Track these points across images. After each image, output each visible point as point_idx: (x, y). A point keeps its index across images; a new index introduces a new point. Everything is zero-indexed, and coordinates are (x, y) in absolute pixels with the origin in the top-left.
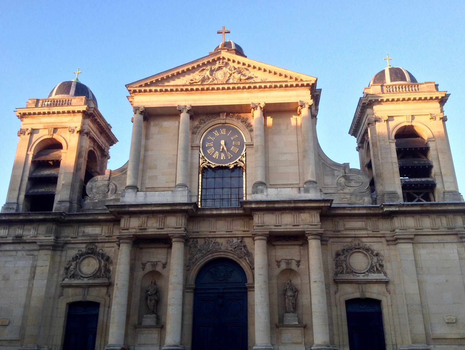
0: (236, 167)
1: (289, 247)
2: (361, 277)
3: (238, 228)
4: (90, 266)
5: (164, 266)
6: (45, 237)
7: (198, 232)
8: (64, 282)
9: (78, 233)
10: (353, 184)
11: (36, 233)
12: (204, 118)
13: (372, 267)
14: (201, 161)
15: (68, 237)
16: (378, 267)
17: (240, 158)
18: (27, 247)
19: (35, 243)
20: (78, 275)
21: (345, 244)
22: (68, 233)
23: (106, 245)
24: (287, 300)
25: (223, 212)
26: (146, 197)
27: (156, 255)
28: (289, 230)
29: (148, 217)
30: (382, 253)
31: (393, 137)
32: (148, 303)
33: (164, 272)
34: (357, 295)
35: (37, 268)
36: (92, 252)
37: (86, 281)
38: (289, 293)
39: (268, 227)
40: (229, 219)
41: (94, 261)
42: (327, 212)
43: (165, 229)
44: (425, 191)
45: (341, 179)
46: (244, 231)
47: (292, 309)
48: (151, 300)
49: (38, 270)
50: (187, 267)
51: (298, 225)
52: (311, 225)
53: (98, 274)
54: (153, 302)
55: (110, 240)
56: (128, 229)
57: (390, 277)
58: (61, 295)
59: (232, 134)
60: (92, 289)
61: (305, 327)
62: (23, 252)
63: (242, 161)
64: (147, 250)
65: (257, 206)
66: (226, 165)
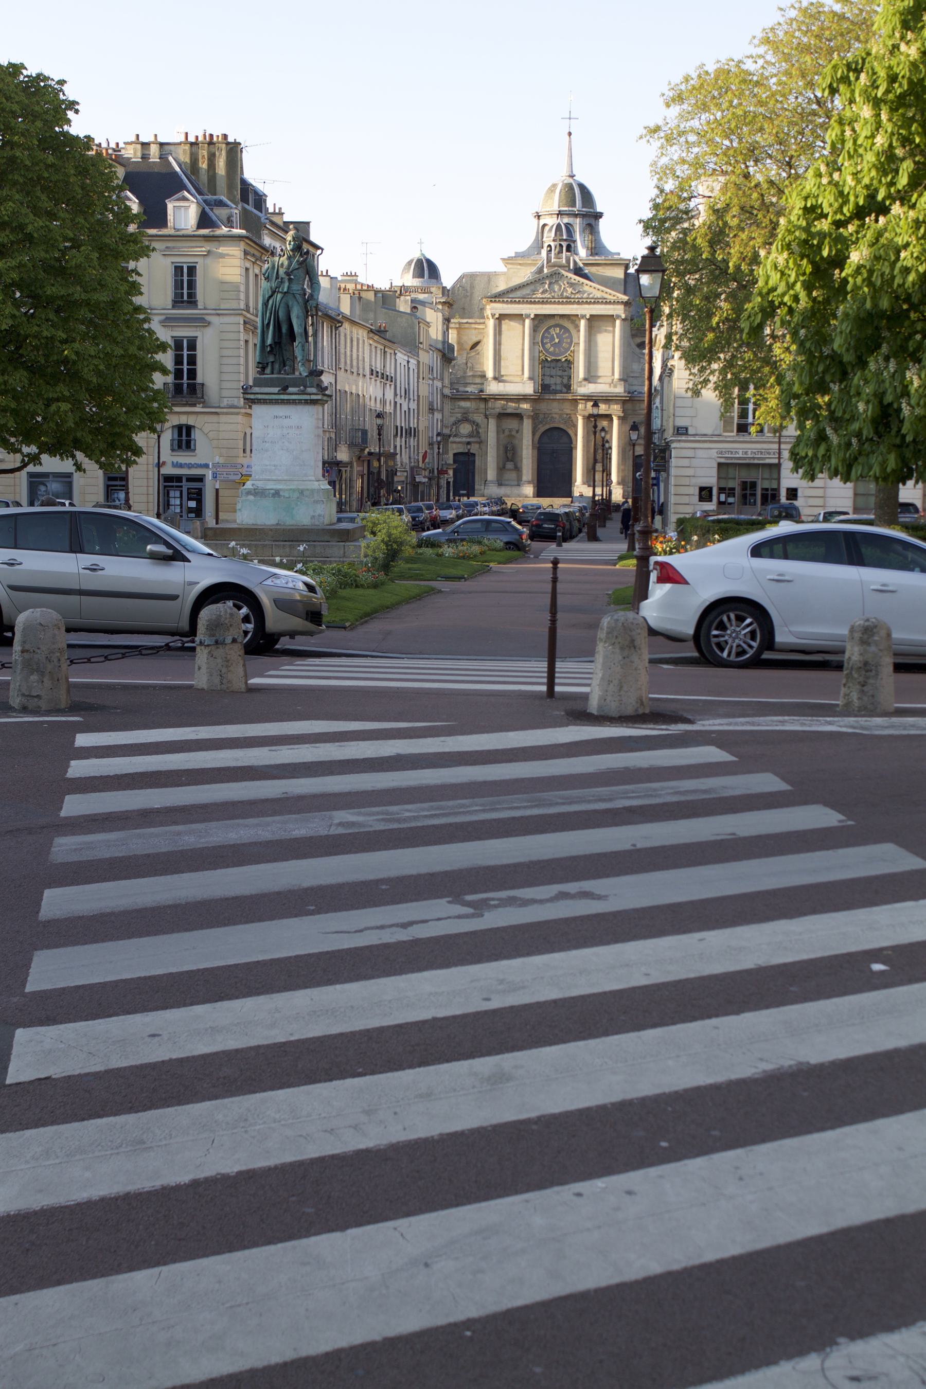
4: (465, 429)
5: (517, 432)
27: (512, 424)
33: (518, 435)
36: (465, 419)
50: (534, 434)
59: (564, 333)
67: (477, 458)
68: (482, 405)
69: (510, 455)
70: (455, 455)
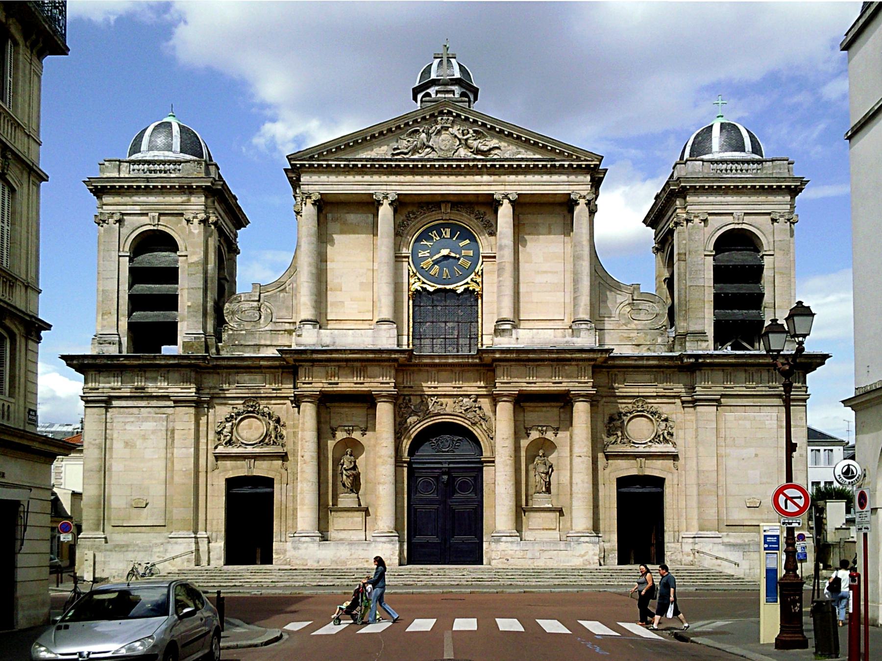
0: (466, 290)
2: (641, 449)
7: (412, 387)
8: (217, 451)
13: (657, 436)
15: (215, 388)
16: (666, 437)
17: (473, 275)
35: (176, 431)
37: (249, 449)
47: (544, 489)
48: (348, 477)
57: (680, 450)
61: (561, 512)
63: (476, 282)
67: (277, 486)
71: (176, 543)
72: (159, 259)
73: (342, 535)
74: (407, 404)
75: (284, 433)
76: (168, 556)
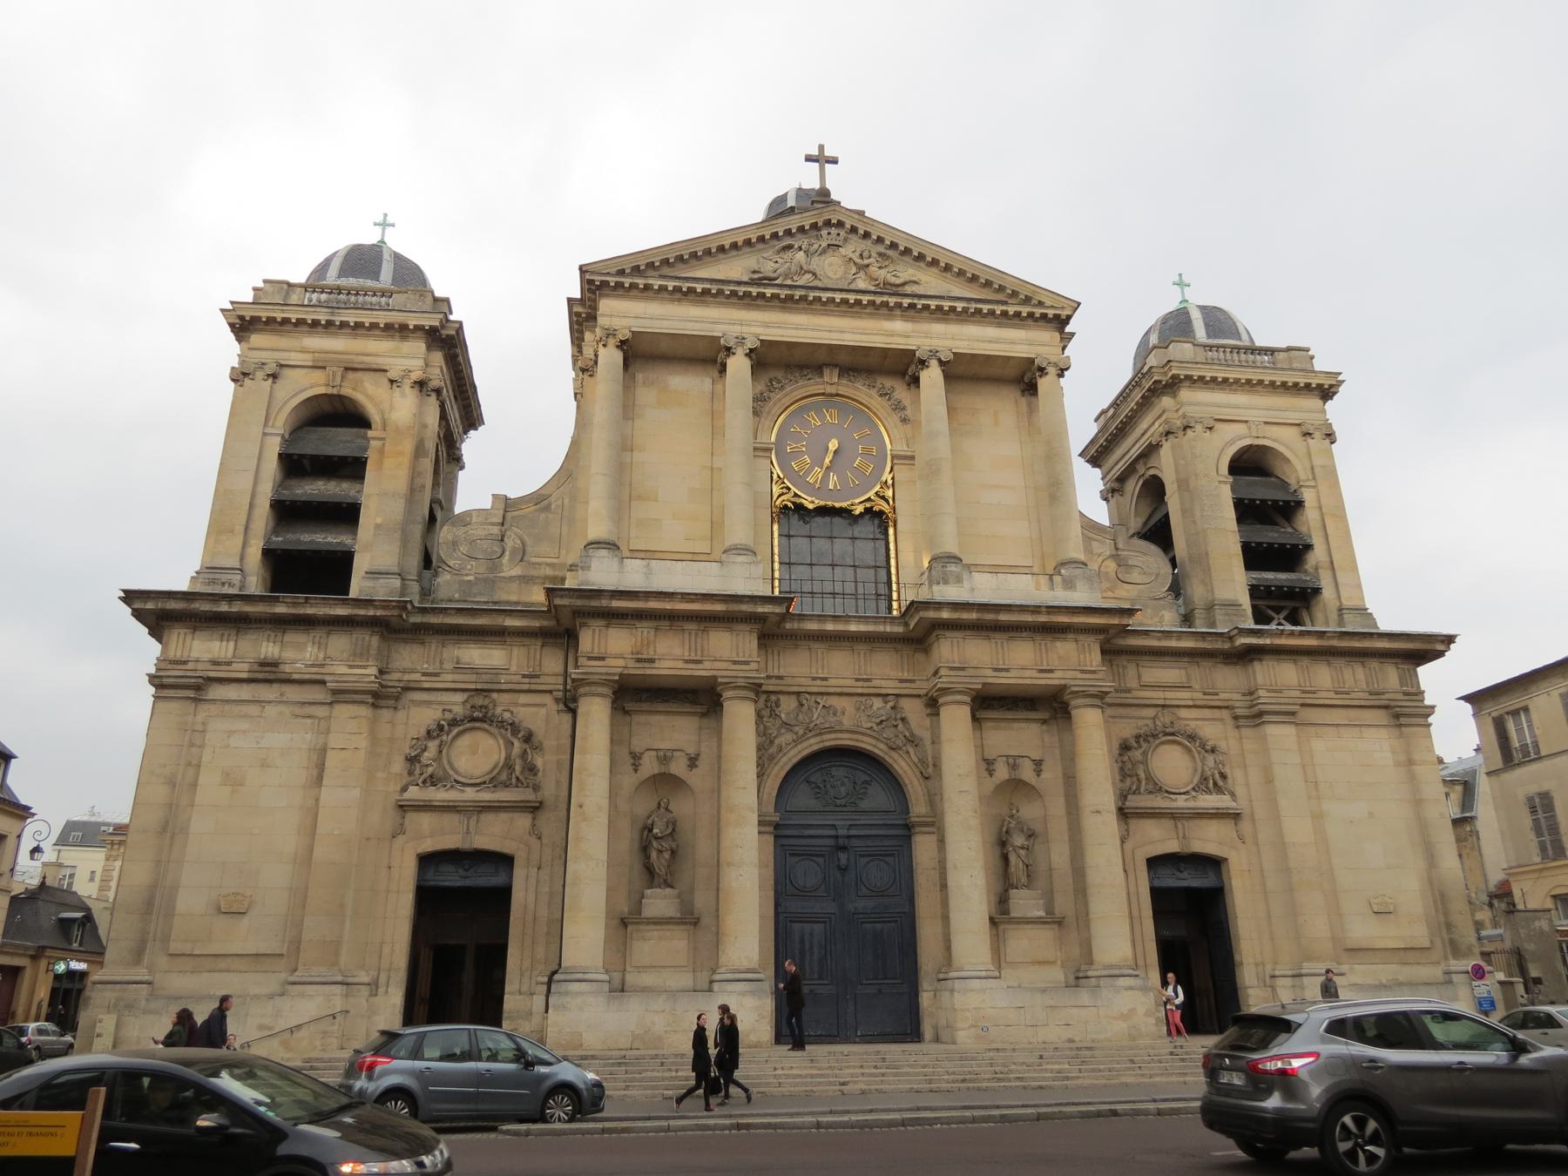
0: (868, 511)
1: (1016, 725)
2: (1181, 802)
3: (885, 670)
4: (477, 754)
5: (693, 762)
6: (351, 667)
7: (780, 678)
8: (407, 795)
9: (441, 663)
10: (1135, 576)
11: (321, 656)
12: (780, 374)
14: (776, 490)
15: (412, 671)
16: (1215, 782)
17: (877, 488)
18: (292, 693)
19: (323, 682)
20: (446, 777)
21: (1140, 723)
22: (410, 660)
23: (523, 698)
24: (1013, 858)
25: (853, 627)
26: (648, 573)
27: (672, 732)
28: (1028, 682)
29: (657, 629)
30: (1222, 745)
31: (1224, 469)
32: (659, 856)
33: (695, 779)
34: (1172, 847)
35: (330, 754)
36: (479, 718)
37: (470, 794)
38: (1019, 840)
39: (979, 672)
40: (862, 648)
41: (491, 741)
42: (1115, 638)
43: (707, 665)
44: (1292, 604)
45: (1108, 563)
46: (902, 681)
48: (660, 851)
49: (332, 760)
51: (1051, 671)
52: (1083, 672)
53: (504, 777)
54: (667, 855)
55: (533, 687)
56: (603, 659)
58: (398, 831)
60: (488, 818)
62: (282, 708)
63: (883, 498)
64: (642, 718)
65: (956, 615)
66: (844, 505)
68: (552, 662)
69: (659, 861)
70: (427, 861)
71: (302, 995)
72: (337, 442)
73: (648, 979)
74: (772, 710)
75: (539, 762)
76: (282, 1024)
